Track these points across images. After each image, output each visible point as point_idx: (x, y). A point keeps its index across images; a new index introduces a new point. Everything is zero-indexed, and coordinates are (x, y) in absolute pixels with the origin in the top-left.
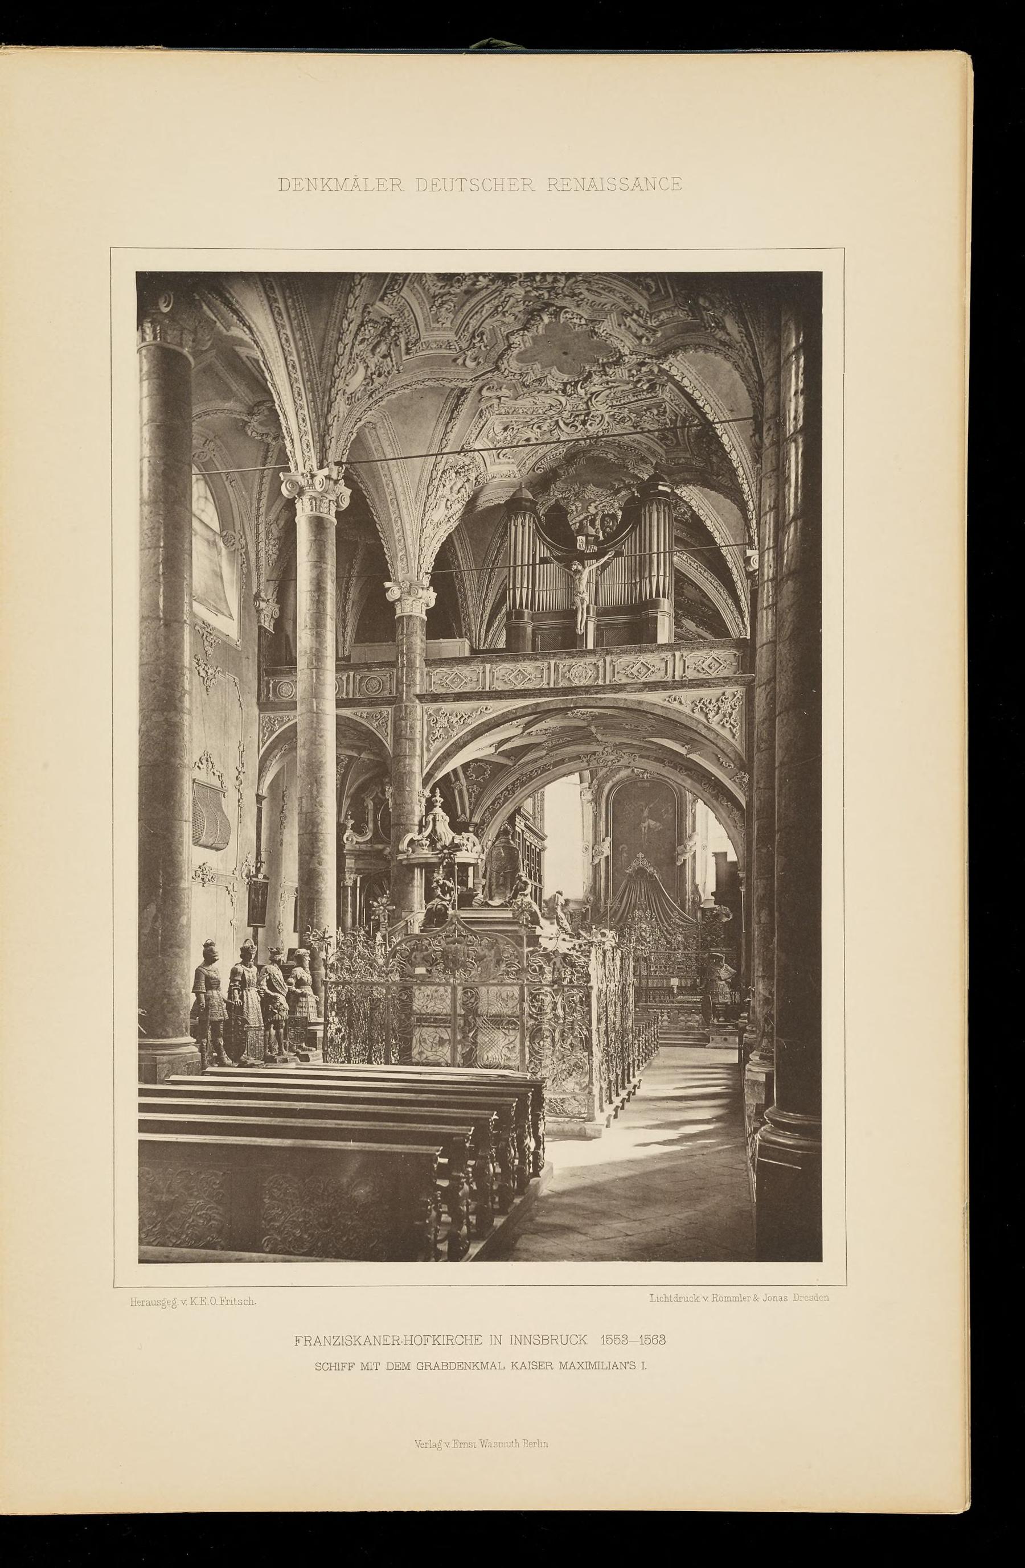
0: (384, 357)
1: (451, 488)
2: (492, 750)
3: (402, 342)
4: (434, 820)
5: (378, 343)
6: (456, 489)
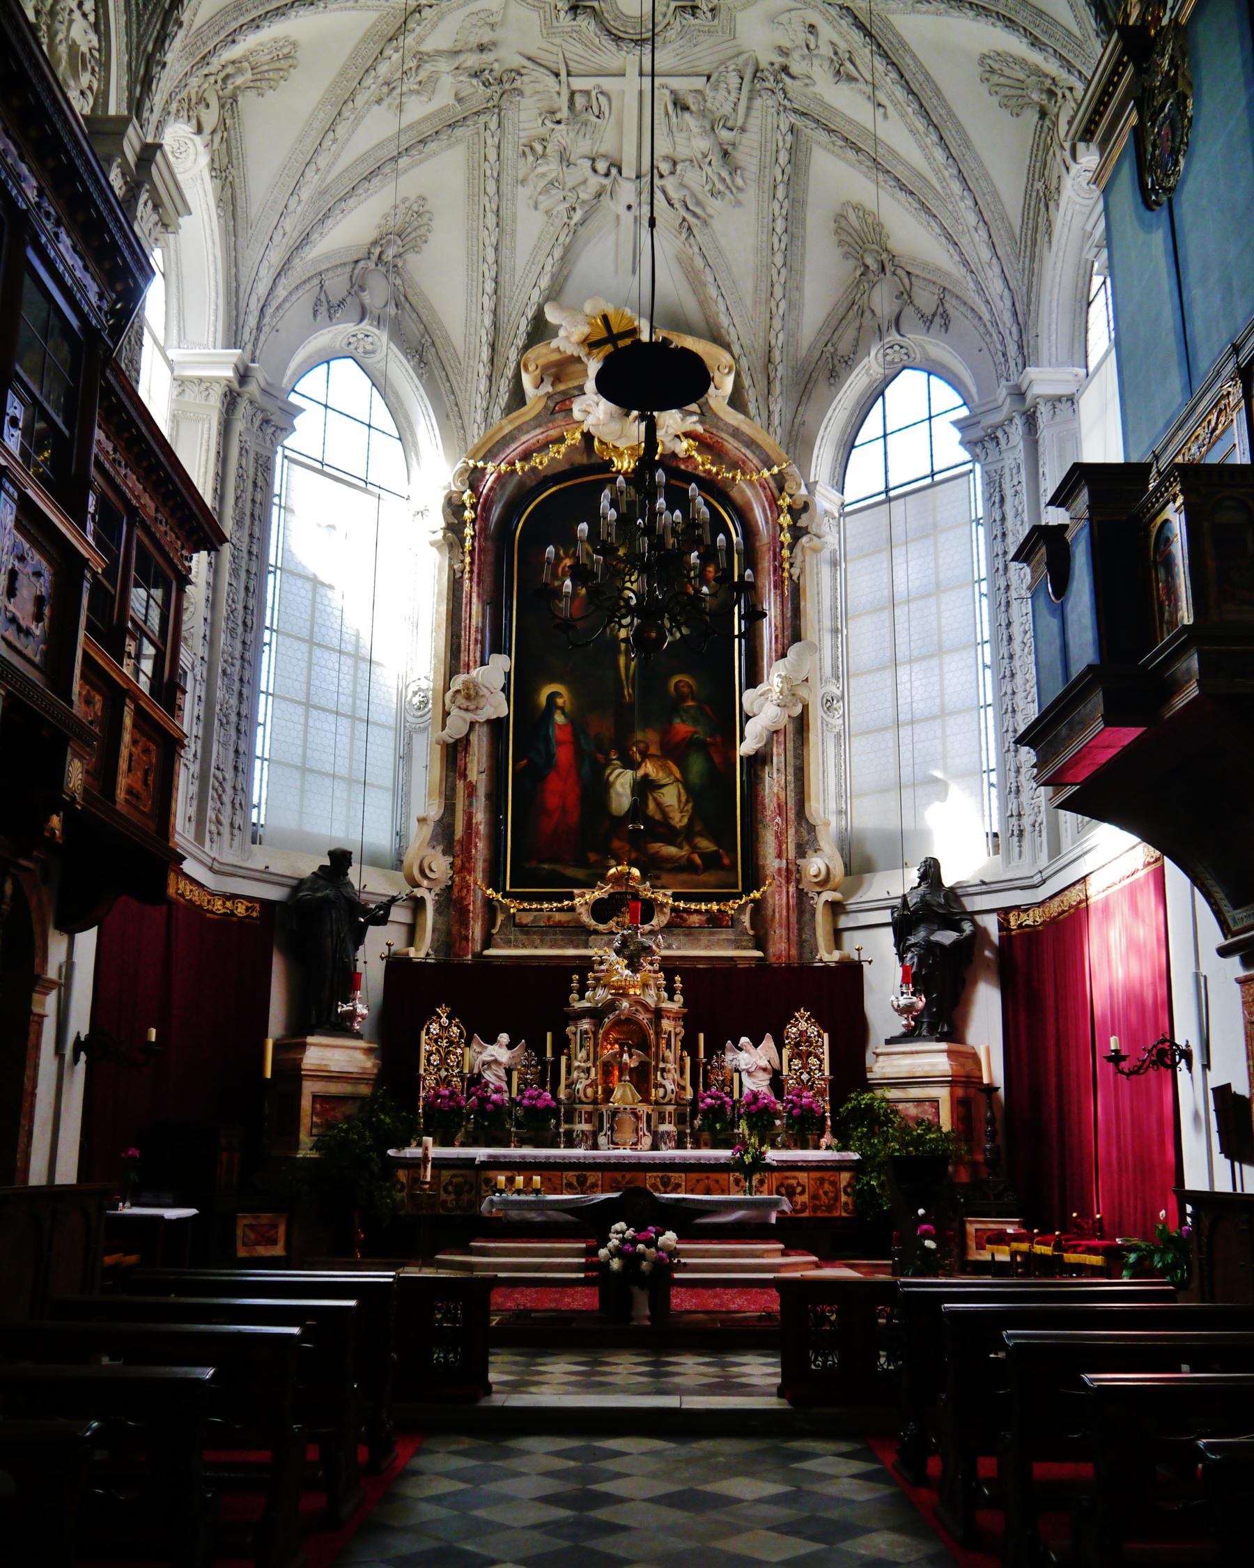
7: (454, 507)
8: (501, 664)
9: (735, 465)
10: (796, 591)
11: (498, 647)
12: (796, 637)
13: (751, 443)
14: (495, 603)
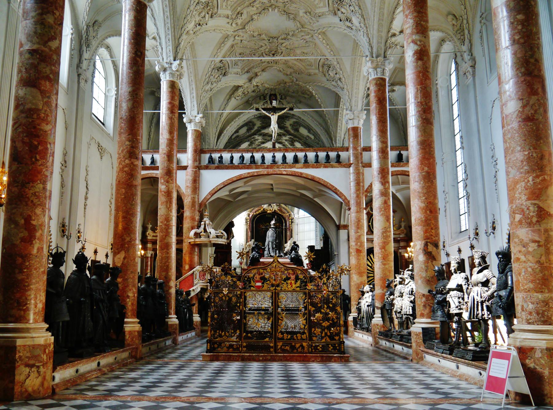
0: (202, 18)
1: (214, 76)
2: (228, 193)
3: (210, 13)
4: (205, 225)
5: (202, 12)
6: (216, 77)
7: (247, 219)
8: (253, 240)
9: (284, 213)
10: (292, 230)
11: (252, 238)
12: (292, 237)
13: (286, 209)
14: (252, 232)
